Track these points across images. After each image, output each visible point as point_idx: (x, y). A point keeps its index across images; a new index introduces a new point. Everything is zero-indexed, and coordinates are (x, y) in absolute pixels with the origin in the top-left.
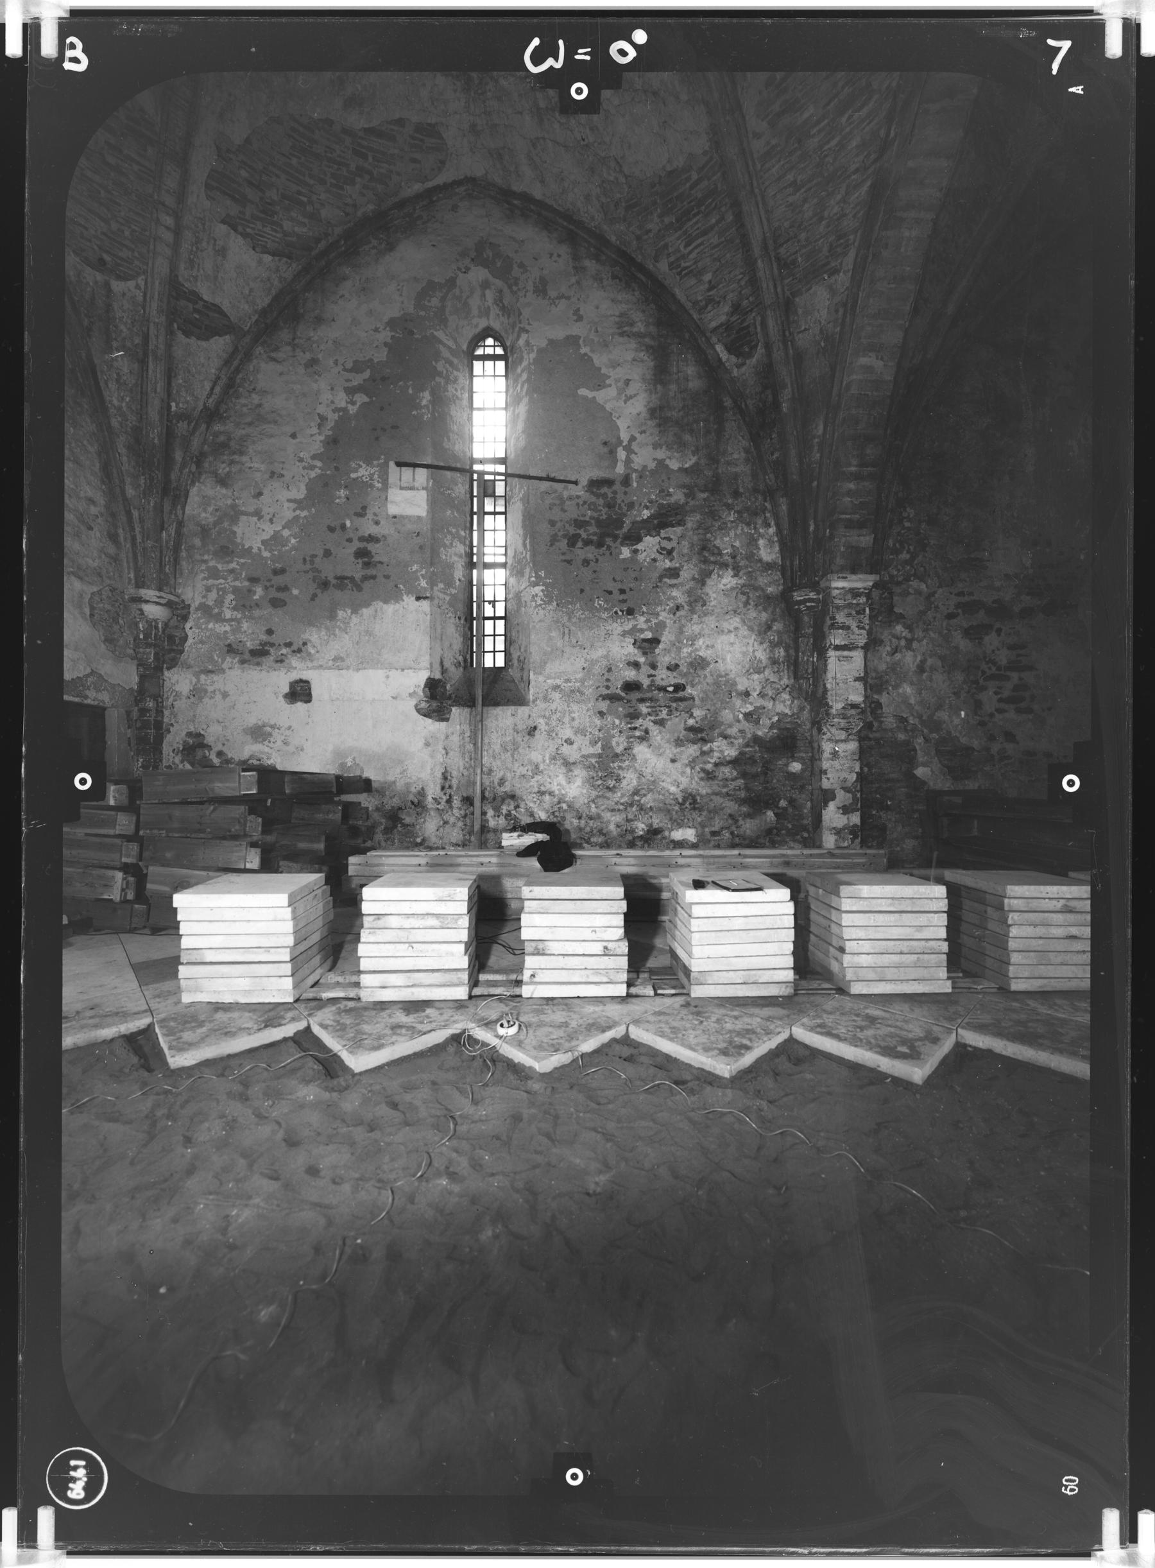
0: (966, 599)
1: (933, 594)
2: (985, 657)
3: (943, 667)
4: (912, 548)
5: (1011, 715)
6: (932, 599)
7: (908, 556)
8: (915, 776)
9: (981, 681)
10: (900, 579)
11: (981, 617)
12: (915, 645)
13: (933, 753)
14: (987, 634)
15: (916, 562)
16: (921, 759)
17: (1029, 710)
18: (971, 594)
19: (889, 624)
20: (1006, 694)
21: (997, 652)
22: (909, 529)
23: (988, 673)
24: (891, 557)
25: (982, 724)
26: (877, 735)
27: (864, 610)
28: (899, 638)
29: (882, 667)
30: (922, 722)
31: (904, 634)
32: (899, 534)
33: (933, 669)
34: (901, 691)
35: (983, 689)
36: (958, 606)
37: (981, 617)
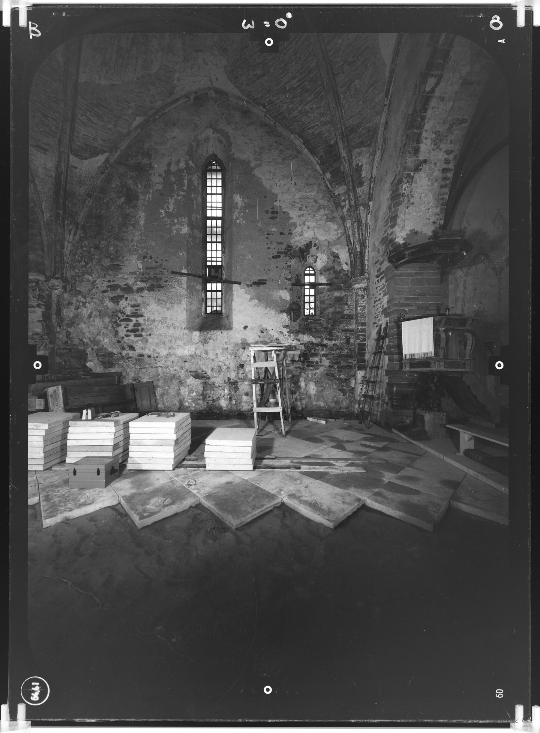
0: (112, 283)
1: (95, 281)
2: (120, 311)
3: (100, 315)
4: (86, 260)
5: (132, 338)
6: (95, 284)
7: (84, 264)
8: (86, 366)
9: (118, 322)
10: (80, 274)
11: (119, 292)
12: (87, 305)
13: (95, 355)
14: (121, 300)
15: (88, 266)
16: (89, 358)
17: (141, 336)
18: (114, 281)
19: (76, 295)
20: (130, 328)
21: (125, 308)
22: (85, 251)
23: (122, 318)
24: (77, 264)
25: (119, 342)
26: (70, 347)
27: (36, 290)
28: (79, 302)
29: (72, 315)
30: (91, 341)
31: (82, 300)
32: (81, 253)
33: (95, 316)
34: (80, 326)
35: (119, 325)
36: (109, 286)
37: (119, 292)
